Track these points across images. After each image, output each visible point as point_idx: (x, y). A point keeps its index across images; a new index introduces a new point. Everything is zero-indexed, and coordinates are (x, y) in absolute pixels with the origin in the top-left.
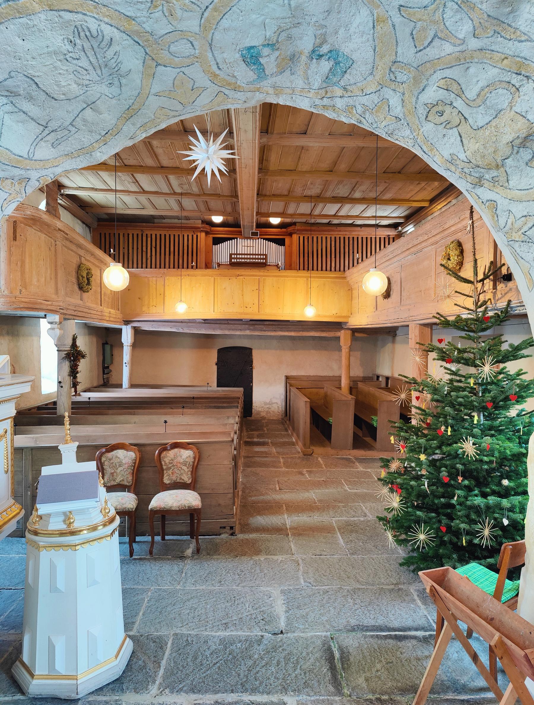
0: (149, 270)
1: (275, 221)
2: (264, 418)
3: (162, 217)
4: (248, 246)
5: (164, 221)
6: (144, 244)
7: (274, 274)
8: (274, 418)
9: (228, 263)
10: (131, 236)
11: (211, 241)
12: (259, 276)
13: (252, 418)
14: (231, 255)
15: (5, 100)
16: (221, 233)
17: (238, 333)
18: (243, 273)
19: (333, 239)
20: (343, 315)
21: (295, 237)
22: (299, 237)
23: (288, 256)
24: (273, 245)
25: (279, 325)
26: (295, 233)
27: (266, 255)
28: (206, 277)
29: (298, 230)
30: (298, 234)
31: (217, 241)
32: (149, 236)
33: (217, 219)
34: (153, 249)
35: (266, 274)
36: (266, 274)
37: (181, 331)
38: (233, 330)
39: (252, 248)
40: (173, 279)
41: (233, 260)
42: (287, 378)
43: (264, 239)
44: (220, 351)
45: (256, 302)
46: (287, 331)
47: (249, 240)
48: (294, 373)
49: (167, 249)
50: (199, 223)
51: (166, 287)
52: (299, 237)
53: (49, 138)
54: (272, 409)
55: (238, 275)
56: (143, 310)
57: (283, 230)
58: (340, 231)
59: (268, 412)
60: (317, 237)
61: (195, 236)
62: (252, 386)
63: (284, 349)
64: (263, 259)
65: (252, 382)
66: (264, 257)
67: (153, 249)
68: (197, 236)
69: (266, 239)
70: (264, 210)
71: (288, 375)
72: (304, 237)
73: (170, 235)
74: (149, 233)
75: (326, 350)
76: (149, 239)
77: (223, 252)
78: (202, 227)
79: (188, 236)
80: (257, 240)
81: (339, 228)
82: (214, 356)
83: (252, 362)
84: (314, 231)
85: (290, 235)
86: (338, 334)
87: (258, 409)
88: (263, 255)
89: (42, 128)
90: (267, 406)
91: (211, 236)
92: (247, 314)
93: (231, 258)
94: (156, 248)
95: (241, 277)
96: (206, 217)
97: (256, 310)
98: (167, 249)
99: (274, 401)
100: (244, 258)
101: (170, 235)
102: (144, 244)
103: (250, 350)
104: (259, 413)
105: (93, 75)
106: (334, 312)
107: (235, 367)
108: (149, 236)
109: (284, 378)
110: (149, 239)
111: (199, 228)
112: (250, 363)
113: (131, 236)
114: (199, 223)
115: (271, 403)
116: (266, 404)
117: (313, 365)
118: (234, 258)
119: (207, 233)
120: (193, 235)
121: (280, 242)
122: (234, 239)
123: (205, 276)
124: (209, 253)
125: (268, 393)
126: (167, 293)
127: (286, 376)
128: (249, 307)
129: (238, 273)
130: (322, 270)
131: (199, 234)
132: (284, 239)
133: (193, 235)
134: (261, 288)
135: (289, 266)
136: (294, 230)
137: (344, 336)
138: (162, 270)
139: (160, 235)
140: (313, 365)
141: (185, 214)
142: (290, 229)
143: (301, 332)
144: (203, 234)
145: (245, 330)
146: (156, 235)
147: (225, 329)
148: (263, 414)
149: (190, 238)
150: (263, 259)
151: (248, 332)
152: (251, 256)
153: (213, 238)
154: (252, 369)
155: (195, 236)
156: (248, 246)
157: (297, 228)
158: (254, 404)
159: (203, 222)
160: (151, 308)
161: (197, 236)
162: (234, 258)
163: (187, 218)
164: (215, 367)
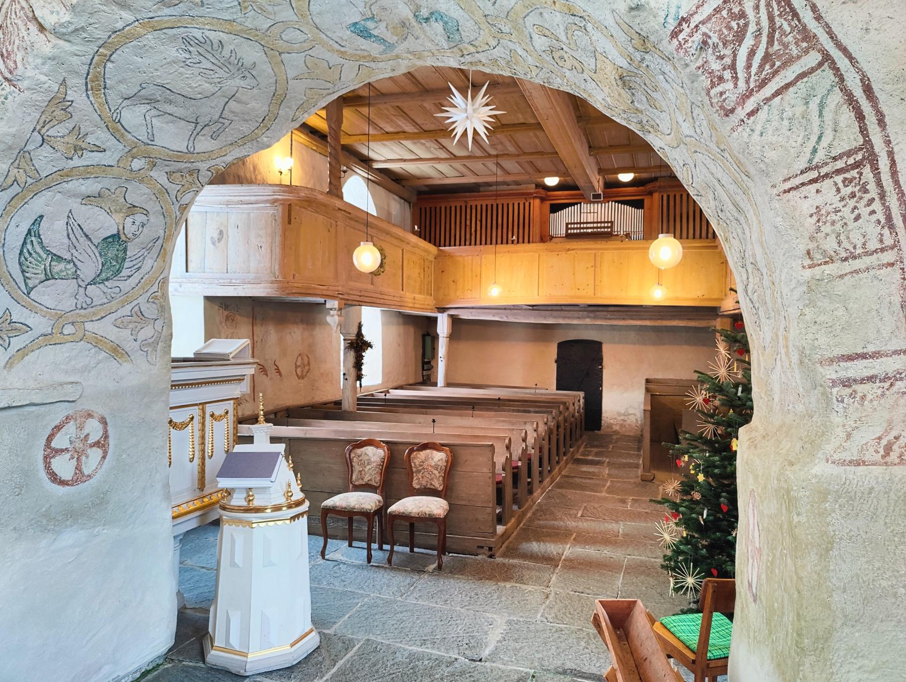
1: (626, 177)
2: (616, 432)
3: (488, 184)
5: (491, 188)
6: (468, 217)
8: (631, 434)
10: (453, 209)
12: (595, 249)
13: (602, 432)
14: (567, 224)
15: (148, 107)
16: (562, 196)
17: (575, 322)
20: (714, 297)
21: (656, 196)
24: (628, 209)
26: (656, 191)
27: (612, 222)
29: (660, 187)
31: (556, 208)
32: (474, 207)
33: (552, 181)
34: (478, 223)
35: (603, 246)
36: (603, 246)
37: (505, 319)
38: (569, 318)
40: (491, 257)
42: (648, 381)
44: (560, 345)
46: (641, 319)
47: (596, 205)
48: (659, 376)
49: (494, 222)
50: (532, 188)
53: (203, 132)
54: (628, 422)
55: (569, 250)
57: (641, 188)
59: (621, 425)
61: (527, 204)
62: (601, 392)
63: (645, 344)
64: (608, 227)
65: (601, 386)
67: (478, 223)
69: (619, 202)
70: (606, 165)
72: (668, 196)
76: (474, 211)
77: (560, 221)
82: (552, 352)
85: (650, 193)
87: (609, 421)
88: (608, 222)
89: (193, 125)
90: (622, 418)
91: (548, 203)
93: (567, 228)
94: (481, 221)
97: (591, 293)
98: (494, 222)
99: (631, 411)
102: (468, 217)
104: (610, 426)
105: (221, 73)
106: (699, 293)
107: (580, 365)
108: (474, 207)
109: (644, 382)
110: (474, 211)
111: (532, 194)
112: (600, 361)
113: (453, 209)
114: (532, 188)
115: (627, 414)
116: (619, 414)
118: (571, 229)
119: (543, 200)
121: (637, 204)
122: (577, 204)
124: (545, 223)
125: (623, 401)
126: (483, 276)
132: (643, 200)
138: (478, 247)
141: (509, 179)
142: (649, 187)
144: (537, 201)
148: (616, 428)
150: (608, 227)
151: (588, 321)
152: (599, 225)
153: (552, 205)
155: (527, 204)
157: (657, 184)
158: (604, 415)
162: (571, 229)
163: (517, 183)
164: (555, 365)
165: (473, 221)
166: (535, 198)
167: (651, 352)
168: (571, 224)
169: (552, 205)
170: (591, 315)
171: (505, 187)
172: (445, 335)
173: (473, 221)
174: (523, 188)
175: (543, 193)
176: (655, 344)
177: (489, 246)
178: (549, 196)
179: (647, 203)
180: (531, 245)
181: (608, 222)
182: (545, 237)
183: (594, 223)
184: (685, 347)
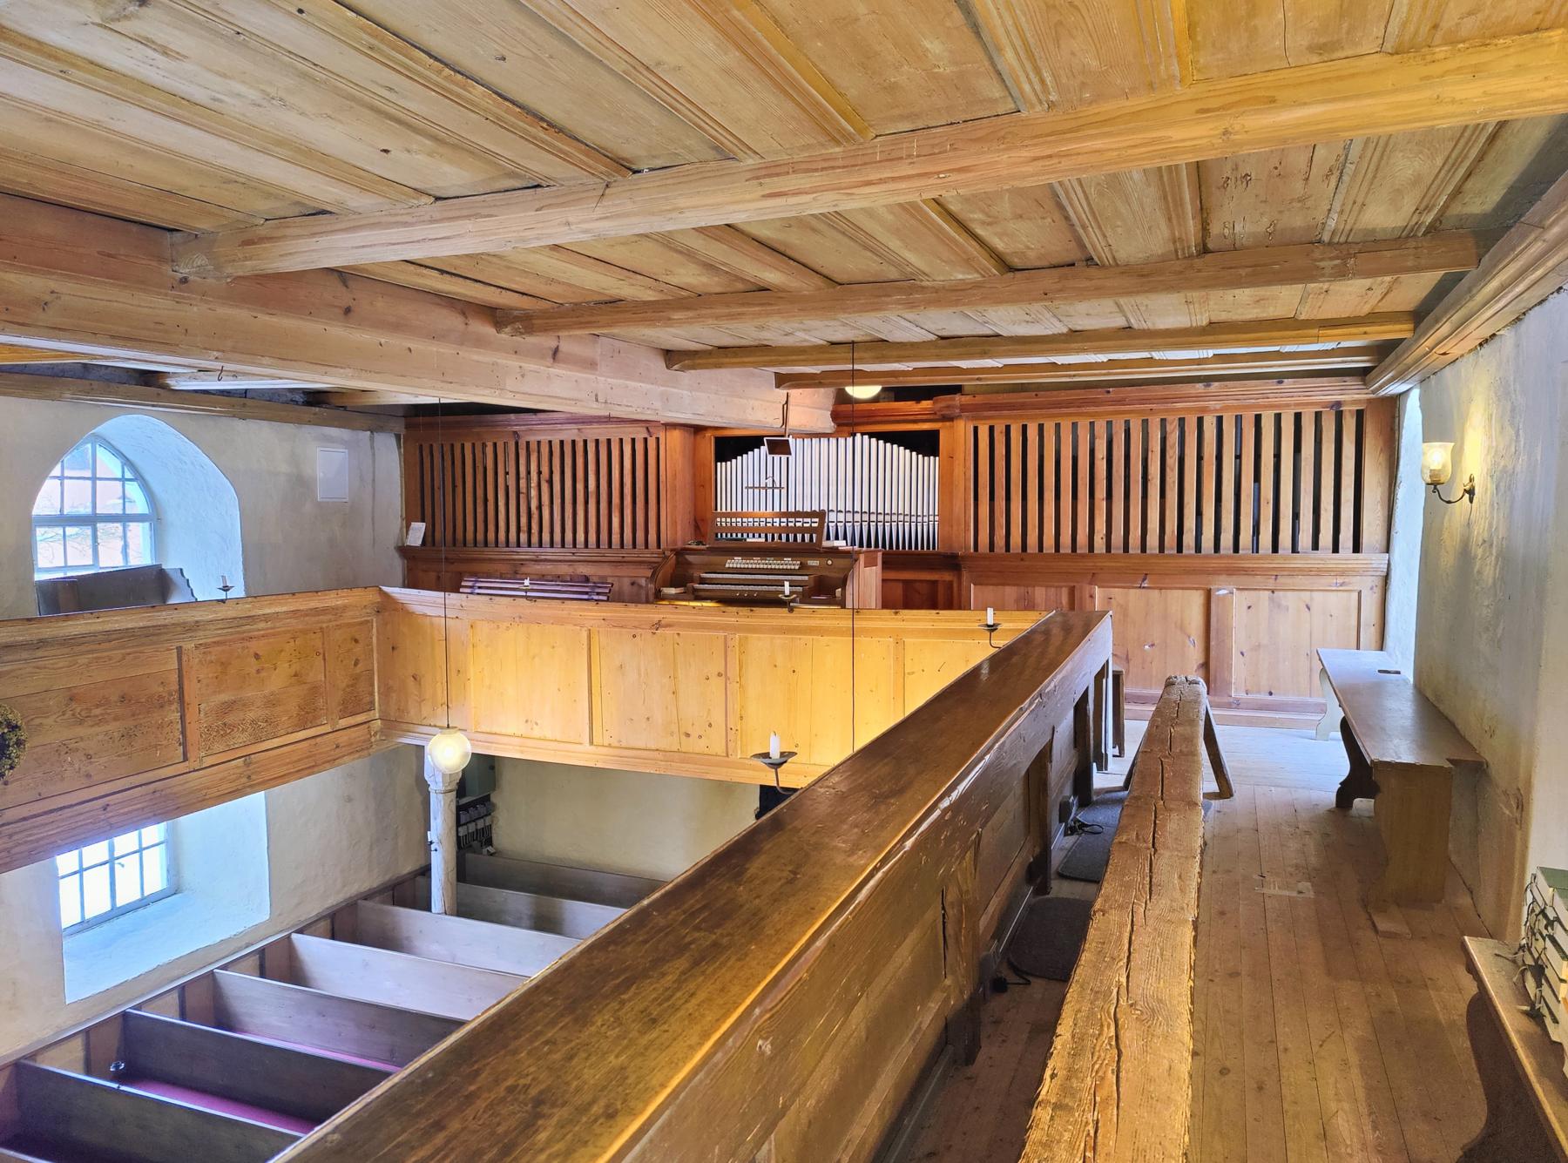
7: (775, 622)
10: (490, 450)
12: (724, 628)
22: (976, 429)
24: (902, 454)
26: (959, 417)
27: (821, 515)
29: (964, 408)
32: (533, 447)
34: (545, 487)
43: (871, 435)
45: (718, 717)
49: (580, 486)
52: (976, 429)
55: (658, 625)
56: (424, 714)
60: (1041, 427)
67: (545, 487)
69: (879, 436)
72: (991, 429)
73: (585, 442)
74: (533, 439)
80: (850, 440)
84: (1023, 406)
88: (812, 514)
95: (668, 632)
97: (719, 748)
98: (580, 486)
113: (490, 450)
121: (925, 444)
123: (560, 621)
128: (694, 735)
129: (656, 617)
132: (934, 435)
134: (733, 672)
142: (943, 401)
150: (811, 530)
153: (718, 440)
156: (766, 488)
165: (534, 484)
169: (718, 440)
172: (441, 787)
173: (534, 484)
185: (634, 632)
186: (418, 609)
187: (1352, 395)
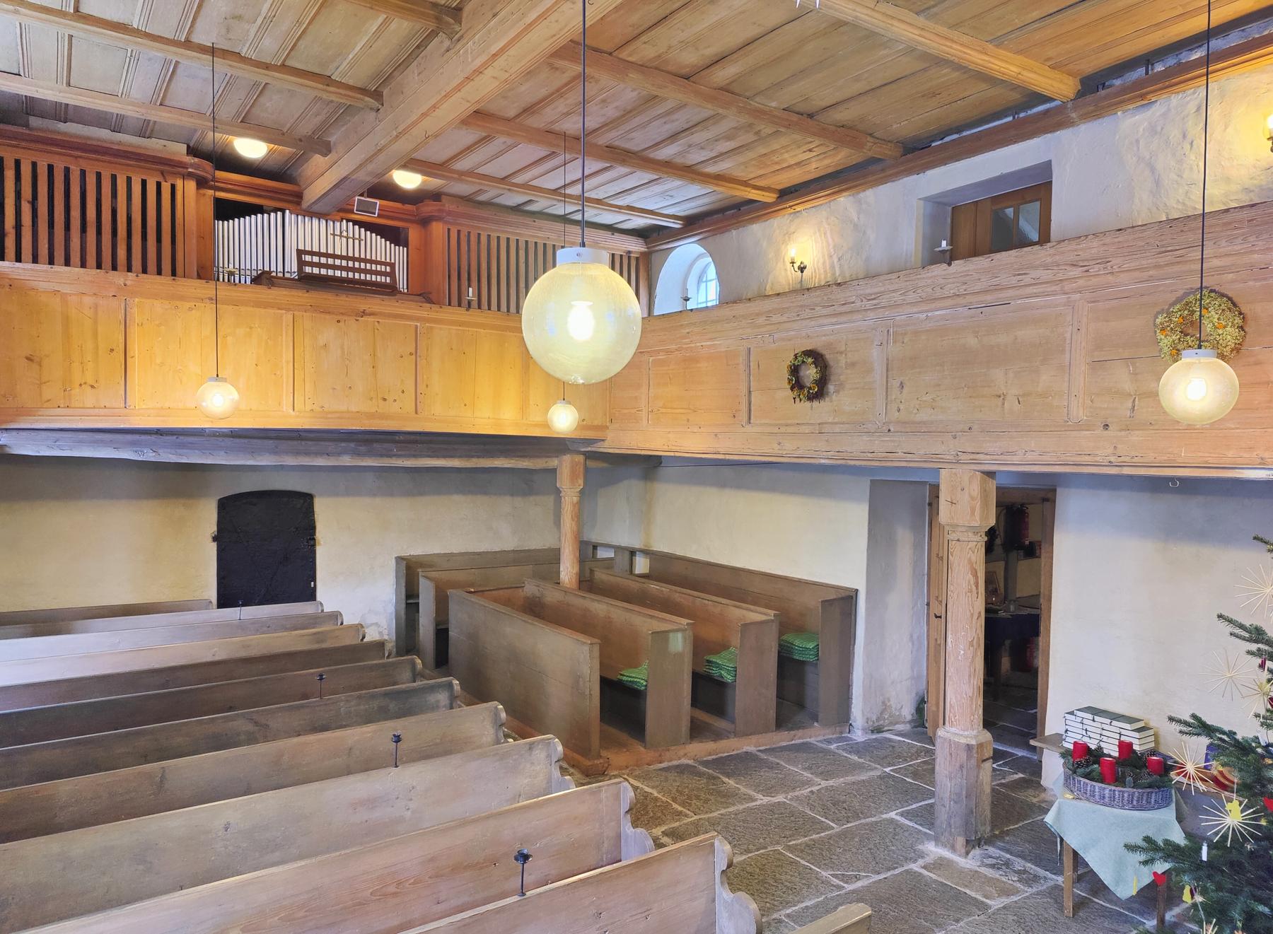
0: (60, 269)
4: (341, 236)
5: (62, 126)
7: (455, 318)
9: (295, 276)
11: (209, 210)
12: (418, 319)
14: (300, 253)
18: (376, 309)
19: (522, 245)
20: (596, 423)
21: (438, 229)
23: (419, 268)
25: (431, 442)
26: (439, 219)
27: (392, 265)
28: (271, 311)
29: (449, 213)
30: (446, 223)
31: (227, 211)
34: (26, 209)
36: (433, 315)
39: (351, 241)
40: (159, 306)
41: (308, 269)
43: (355, 223)
44: (225, 506)
46: (444, 457)
48: (417, 549)
50: (178, 150)
51: (134, 332)
55: (364, 313)
58: (540, 229)
65: (314, 580)
66: (388, 269)
67: (26, 209)
68: (173, 187)
71: (403, 554)
72: (459, 232)
73: (83, 173)
75: (485, 493)
78: (192, 165)
79: (144, 183)
81: (539, 223)
82: (207, 518)
83: (314, 528)
85: (425, 222)
86: (553, 463)
88: (385, 264)
92: (383, 417)
93: (301, 263)
95: (370, 319)
96: (211, 138)
97: (410, 407)
100: (327, 266)
101: (83, 173)
103: (307, 499)
112: (308, 530)
114: (178, 150)
117: (457, 529)
118: (312, 264)
119: (202, 183)
120: (159, 185)
122: (276, 210)
123: (266, 305)
124: (208, 241)
126: (135, 349)
127: (399, 559)
129: (362, 307)
130: (479, 307)
131: (179, 183)
133: (159, 185)
135: (424, 294)
136: (440, 210)
137: (566, 465)
138: (119, 278)
139: (51, 168)
140: (457, 529)
143: (474, 460)
144: (191, 185)
145: (339, 454)
146: (34, 165)
147: (287, 452)
149: (137, 189)
152: (323, 260)
153: (219, 203)
154: (314, 545)
155: (166, 188)
159: (192, 151)
160: (77, 391)
161: (173, 187)
162: (312, 264)
166: (191, 175)
167: (401, 510)
168: (312, 253)
170: (363, 449)
171: (104, 134)
174: (154, 145)
175: (206, 168)
176: (408, 494)
177: (151, 280)
178: (214, 179)
179: (414, 234)
180: (181, 281)
181: (385, 264)
182: (206, 271)
183: (347, 258)
184: (456, 498)
185: (339, 318)
186: (43, 286)
187: (636, 246)
